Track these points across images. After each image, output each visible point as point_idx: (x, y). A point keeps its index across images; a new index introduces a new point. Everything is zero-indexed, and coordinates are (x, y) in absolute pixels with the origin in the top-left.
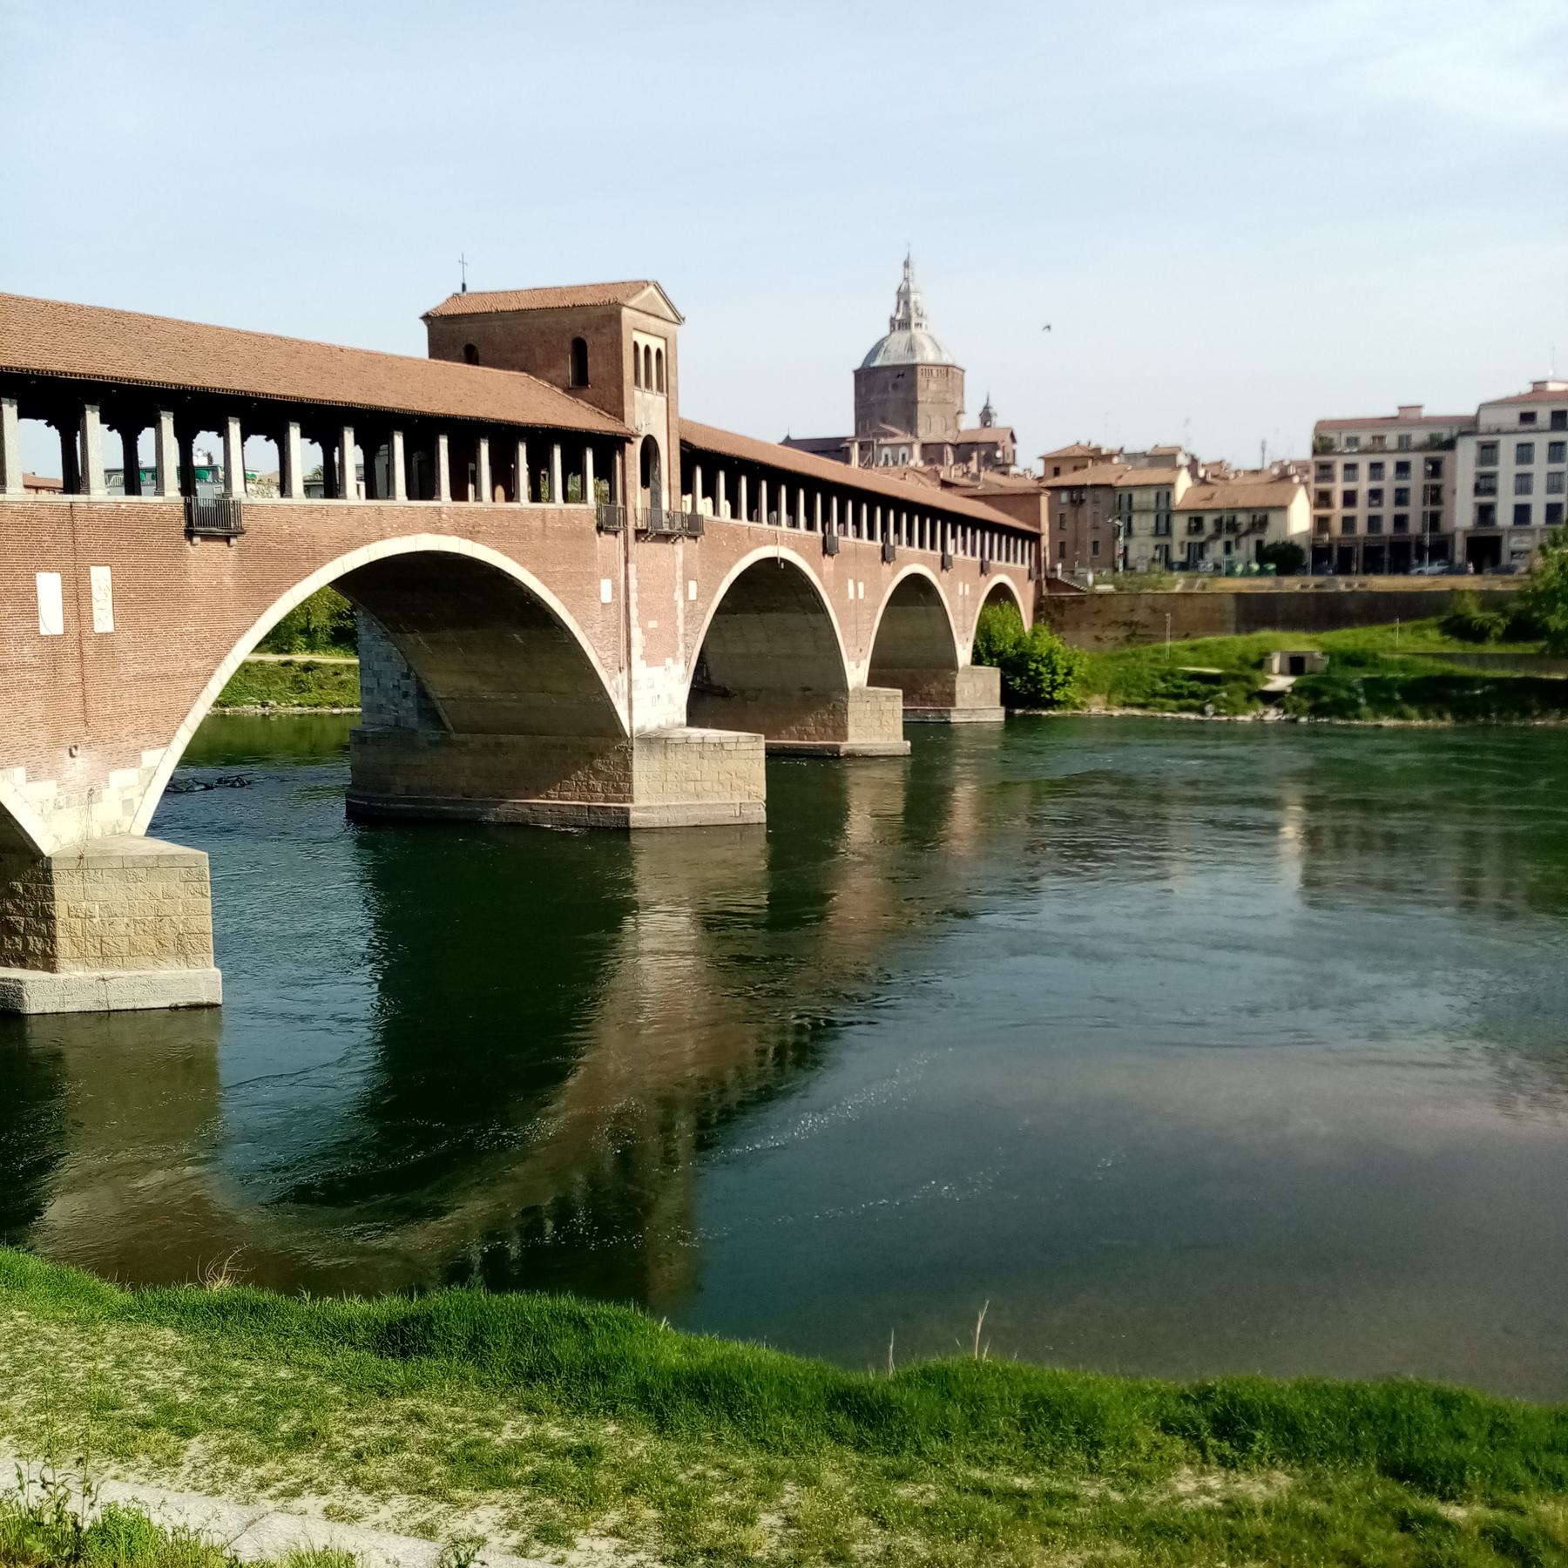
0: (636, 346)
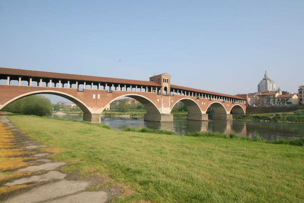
0: (164, 79)
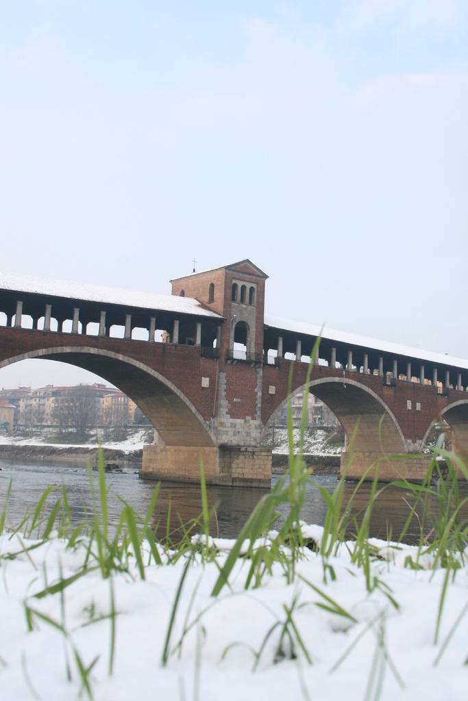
0: (235, 286)
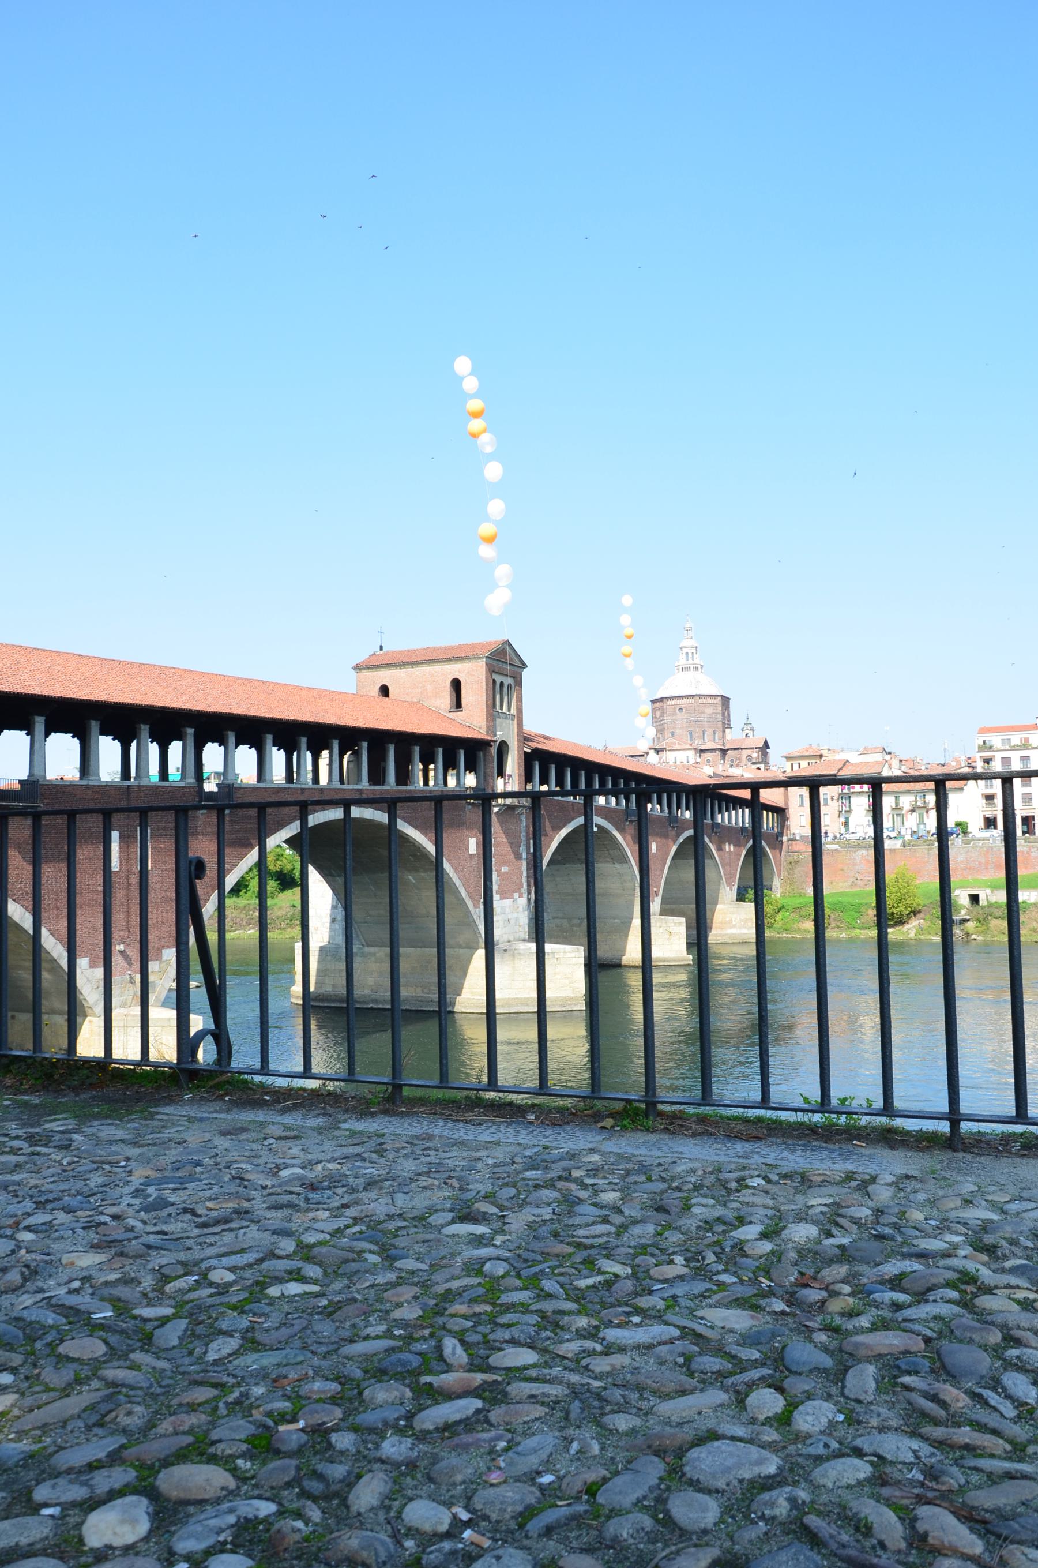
0: (494, 681)
